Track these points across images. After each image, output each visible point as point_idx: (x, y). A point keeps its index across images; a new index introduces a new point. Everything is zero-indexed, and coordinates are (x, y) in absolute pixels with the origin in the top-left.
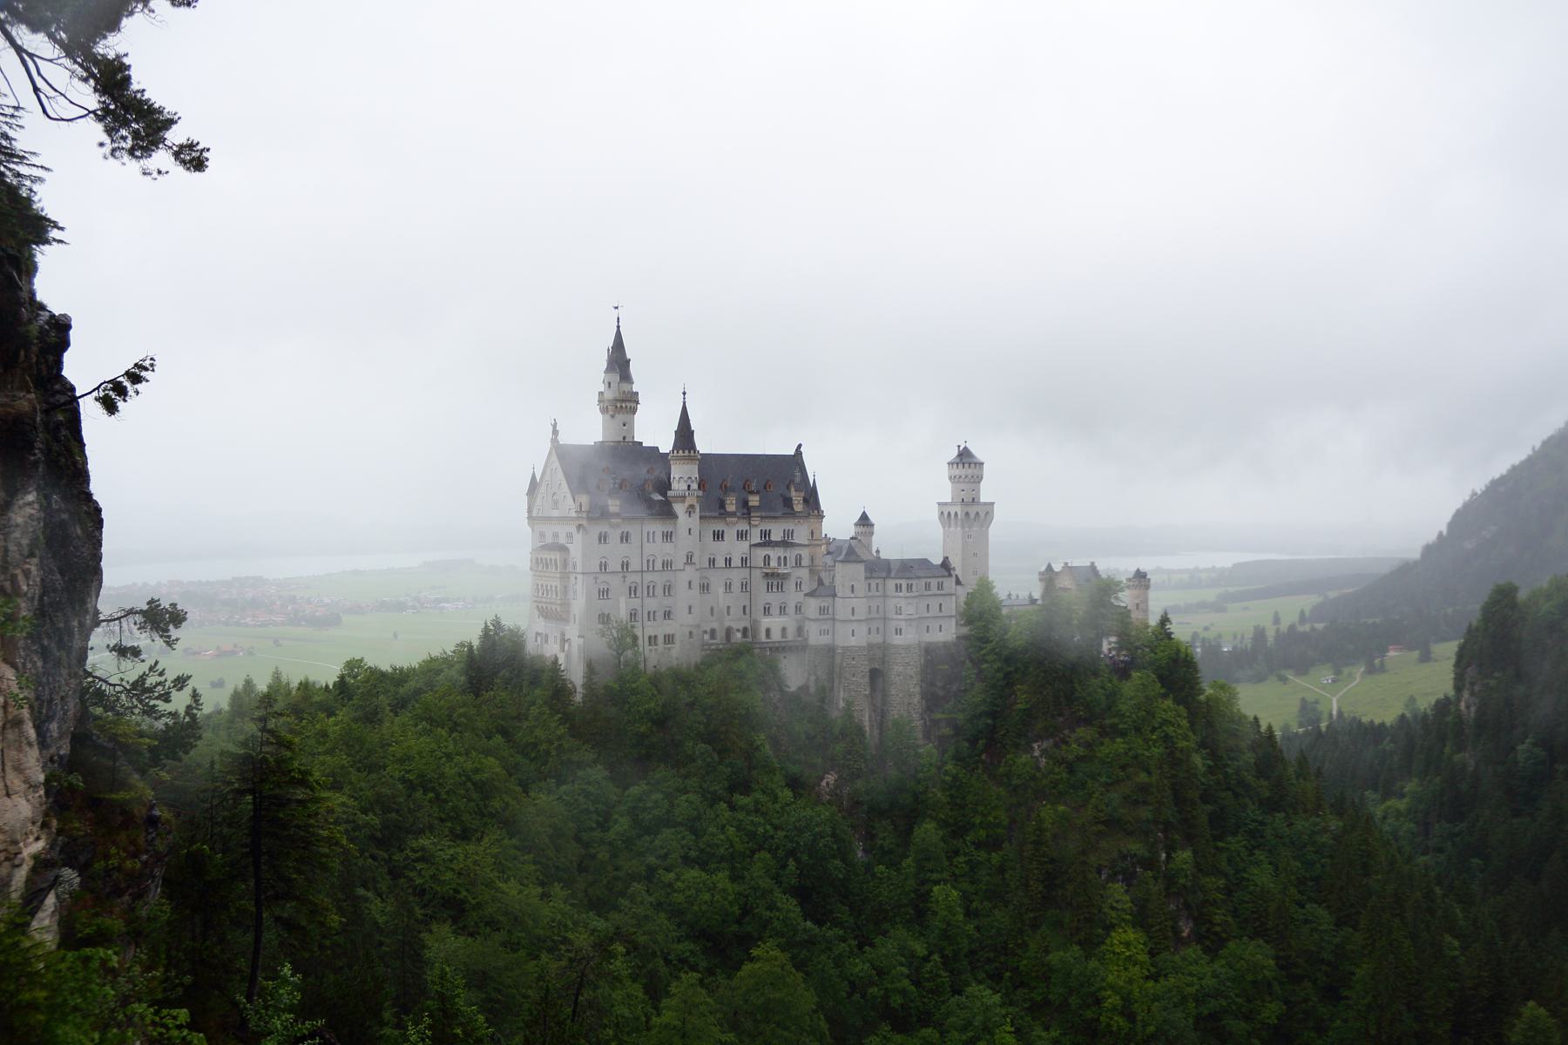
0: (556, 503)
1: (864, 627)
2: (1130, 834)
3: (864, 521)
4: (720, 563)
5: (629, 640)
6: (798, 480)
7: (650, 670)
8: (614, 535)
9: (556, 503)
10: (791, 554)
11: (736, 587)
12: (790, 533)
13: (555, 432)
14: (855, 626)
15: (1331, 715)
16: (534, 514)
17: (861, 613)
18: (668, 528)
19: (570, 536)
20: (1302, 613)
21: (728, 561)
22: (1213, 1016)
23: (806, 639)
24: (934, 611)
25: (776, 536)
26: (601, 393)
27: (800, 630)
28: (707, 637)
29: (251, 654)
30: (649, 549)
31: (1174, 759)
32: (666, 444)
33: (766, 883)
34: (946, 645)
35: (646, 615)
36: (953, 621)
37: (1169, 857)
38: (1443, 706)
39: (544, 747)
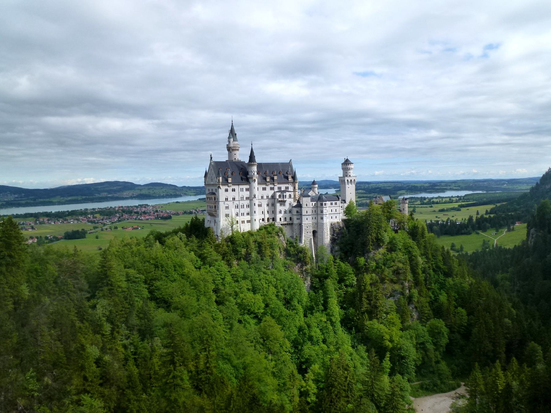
0: (212, 179)
1: (311, 217)
2: (395, 283)
3: (314, 183)
4: (265, 197)
5: (235, 222)
6: (290, 171)
7: (242, 231)
8: (230, 189)
9: (212, 179)
10: (287, 194)
11: (270, 205)
12: (287, 188)
13: (211, 158)
14: (307, 217)
15: (493, 246)
16: (206, 183)
17: (310, 212)
18: (248, 187)
19: (216, 190)
20: (487, 211)
21: (268, 197)
22: (423, 343)
23: (293, 221)
24: (334, 211)
25: (283, 189)
26: (227, 145)
27: (291, 219)
28: (261, 221)
29: (143, 228)
30: (241, 194)
31: (412, 259)
32: (247, 160)
33: (274, 297)
34: (338, 222)
35: (241, 214)
36: (341, 215)
37: (409, 291)
38: (524, 243)
39: (206, 255)
